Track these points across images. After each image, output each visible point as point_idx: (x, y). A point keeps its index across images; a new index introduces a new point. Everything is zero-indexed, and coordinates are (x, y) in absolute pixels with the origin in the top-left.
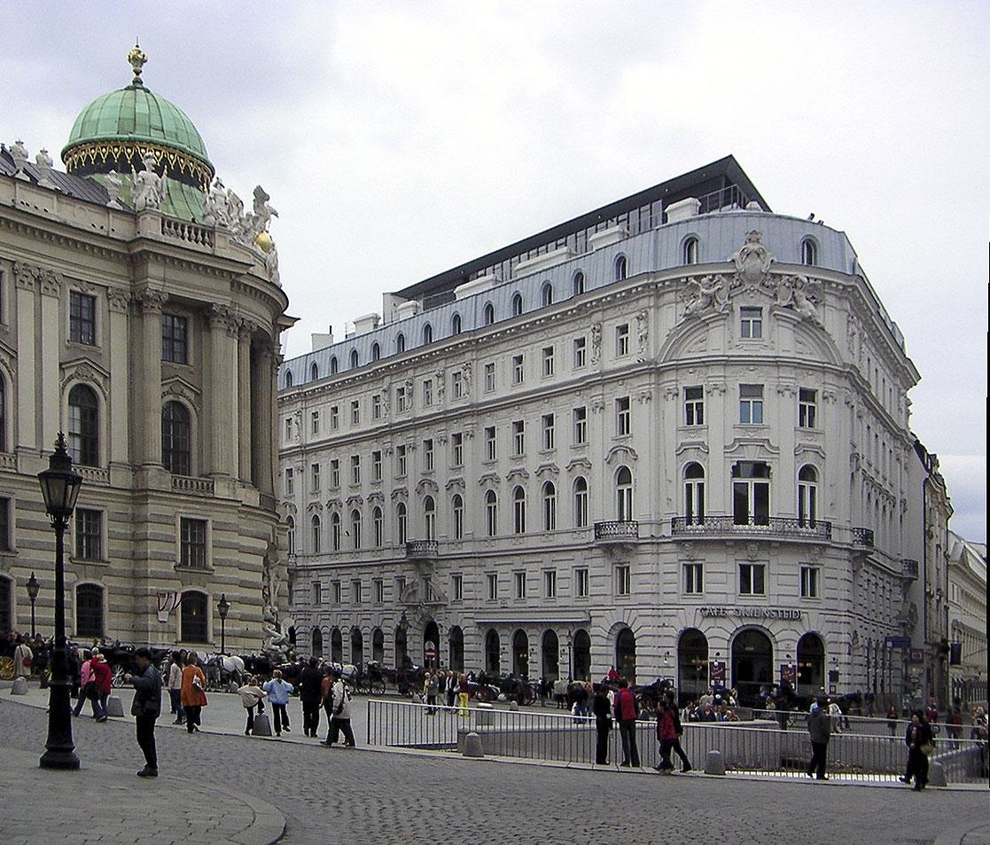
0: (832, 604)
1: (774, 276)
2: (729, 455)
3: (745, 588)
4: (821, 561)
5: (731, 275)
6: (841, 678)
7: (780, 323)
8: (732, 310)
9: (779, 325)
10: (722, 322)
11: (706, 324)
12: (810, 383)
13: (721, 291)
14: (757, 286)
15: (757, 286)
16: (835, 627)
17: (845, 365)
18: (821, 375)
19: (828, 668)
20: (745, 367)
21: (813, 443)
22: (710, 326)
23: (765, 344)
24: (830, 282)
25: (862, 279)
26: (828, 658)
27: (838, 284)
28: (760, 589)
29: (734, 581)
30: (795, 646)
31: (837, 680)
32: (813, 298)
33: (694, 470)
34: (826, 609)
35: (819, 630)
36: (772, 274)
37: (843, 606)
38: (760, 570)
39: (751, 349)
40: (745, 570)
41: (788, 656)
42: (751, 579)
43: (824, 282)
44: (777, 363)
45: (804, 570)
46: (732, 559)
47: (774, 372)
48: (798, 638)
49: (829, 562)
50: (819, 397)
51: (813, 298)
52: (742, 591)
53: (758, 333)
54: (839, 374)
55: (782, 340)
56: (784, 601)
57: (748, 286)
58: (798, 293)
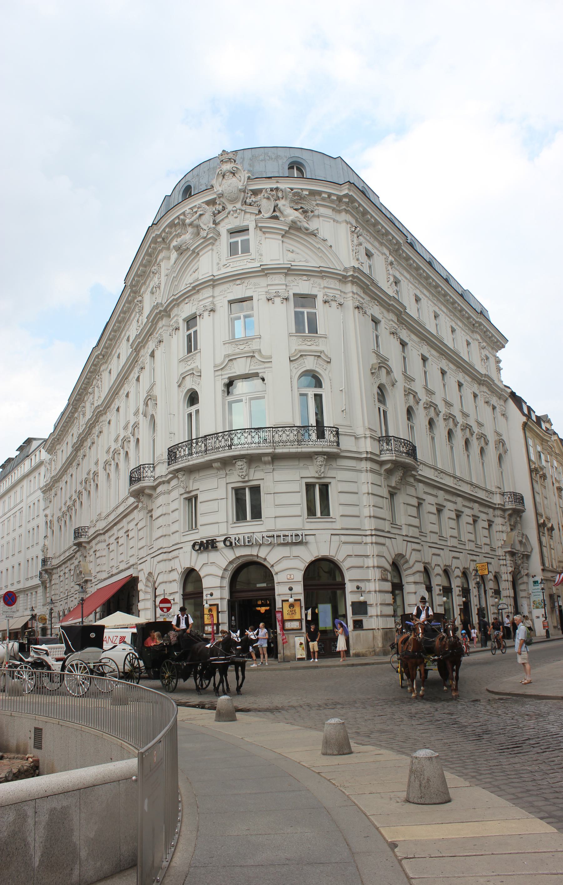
0: (352, 523)
1: (255, 193)
2: (219, 373)
3: (240, 516)
4: (331, 473)
5: (212, 202)
6: (372, 611)
7: (267, 235)
8: (219, 235)
9: (266, 238)
10: (210, 247)
11: (196, 253)
12: (303, 286)
13: (203, 218)
14: (239, 205)
15: (239, 205)
16: (359, 550)
17: (346, 270)
18: (319, 280)
19: (350, 598)
20: (231, 284)
21: (313, 348)
22: (200, 254)
23: (253, 257)
24: (319, 193)
25: (365, 192)
26: (349, 587)
27: (330, 195)
28: (257, 514)
29: (227, 507)
30: (299, 576)
31: (365, 613)
32: (302, 208)
33: (193, 398)
34: (342, 529)
35: (334, 555)
36: (251, 190)
37: (369, 525)
38: (256, 490)
39: (241, 264)
40: (239, 493)
41: (291, 589)
42: (248, 504)
43: (313, 193)
44: (265, 272)
45: (310, 487)
46: (223, 482)
47: (263, 281)
48: (303, 566)
49: (341, 475)
50: (319, 301)
51: (302, 208)
52: (238, 519)
53: (246, 250)
54: (343, 279)
55: (270, 250)
56: (282, 524)
57: (230, 207)
58: (281, 203)
